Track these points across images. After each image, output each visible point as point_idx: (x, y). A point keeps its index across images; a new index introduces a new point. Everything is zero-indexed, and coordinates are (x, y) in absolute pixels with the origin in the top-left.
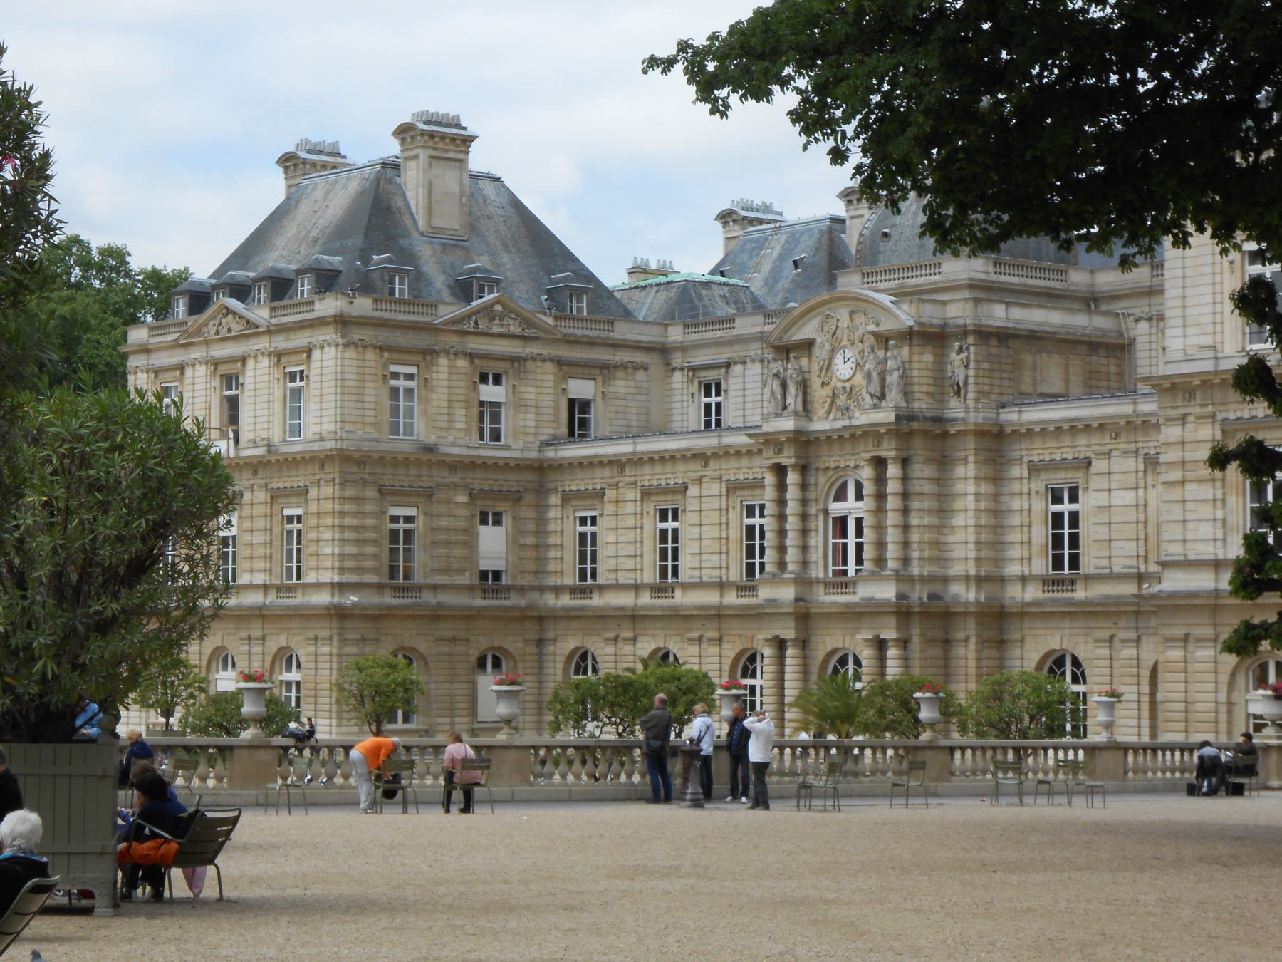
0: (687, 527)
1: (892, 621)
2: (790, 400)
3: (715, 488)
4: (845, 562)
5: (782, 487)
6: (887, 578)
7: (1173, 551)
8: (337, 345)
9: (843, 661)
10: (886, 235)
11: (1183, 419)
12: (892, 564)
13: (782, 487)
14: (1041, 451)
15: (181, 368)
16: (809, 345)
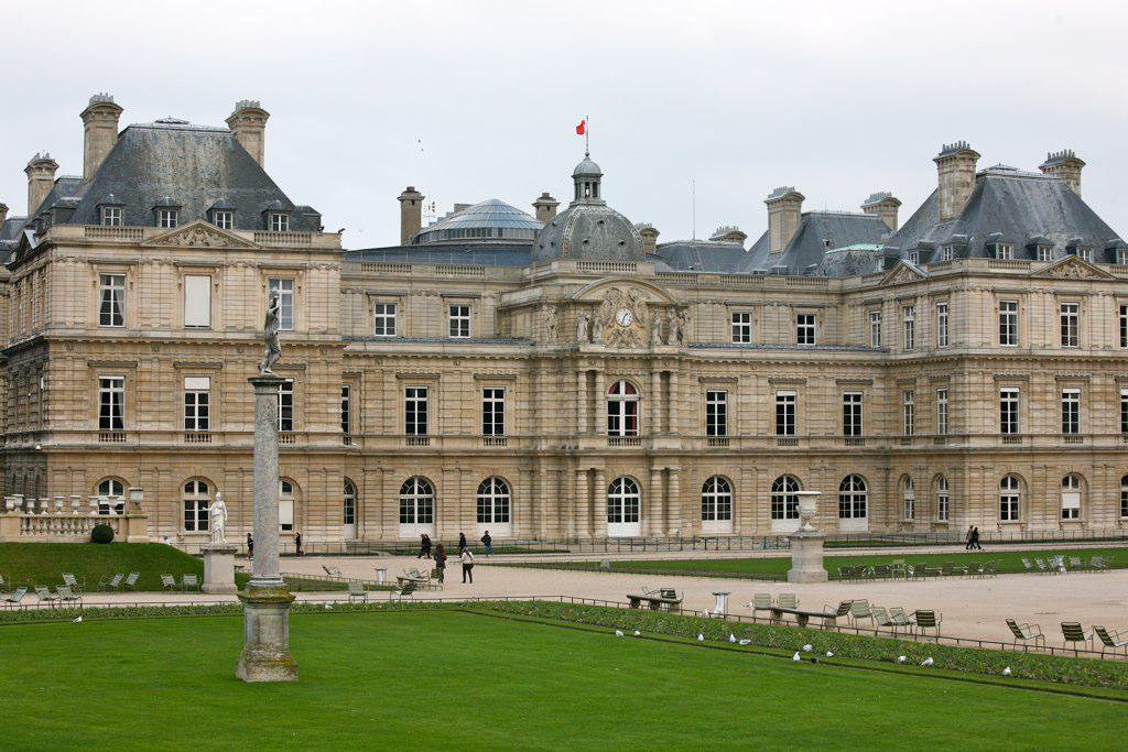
0: (432, 402)
1: (677, 461)
2: (598, 335)
3: (469, 379)
4: (618, 427)
5: (592, 383)
6: (675, 437)
7: (973, 430)
8: (336, 269)
9: (620, 480)
10: (586, 242)
11: (977, 373)
12: (674, 430)
13: (592, 383)
14: (707, 372)
15: (135, 263)
16: (599, 303)
